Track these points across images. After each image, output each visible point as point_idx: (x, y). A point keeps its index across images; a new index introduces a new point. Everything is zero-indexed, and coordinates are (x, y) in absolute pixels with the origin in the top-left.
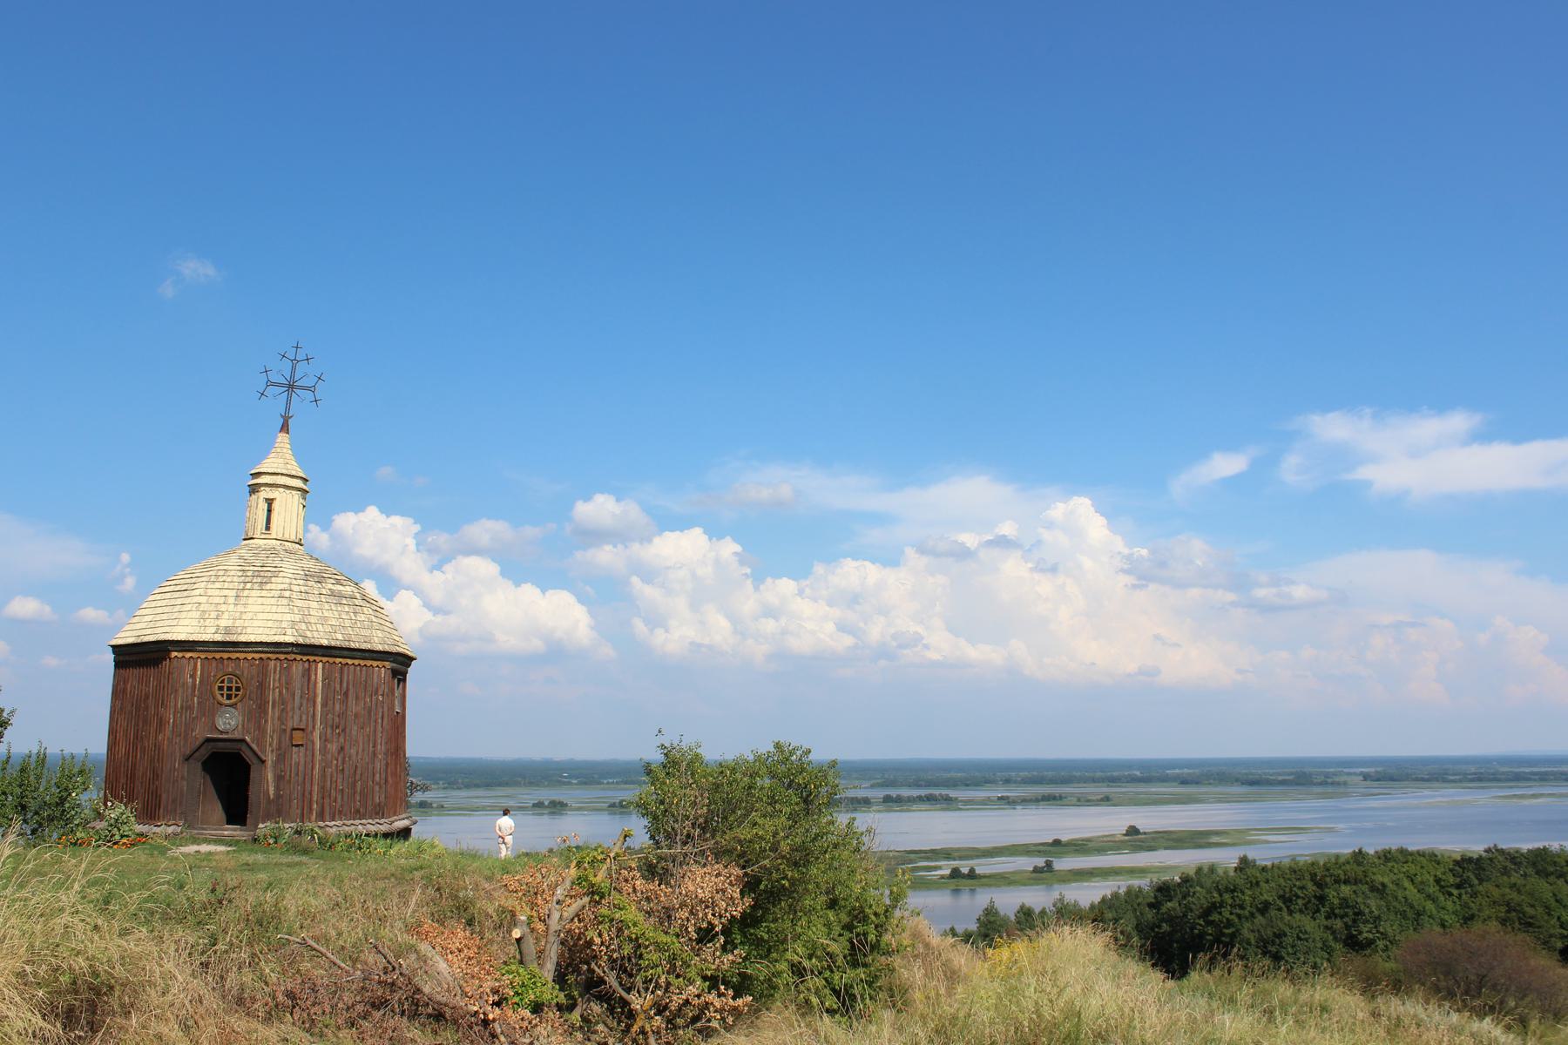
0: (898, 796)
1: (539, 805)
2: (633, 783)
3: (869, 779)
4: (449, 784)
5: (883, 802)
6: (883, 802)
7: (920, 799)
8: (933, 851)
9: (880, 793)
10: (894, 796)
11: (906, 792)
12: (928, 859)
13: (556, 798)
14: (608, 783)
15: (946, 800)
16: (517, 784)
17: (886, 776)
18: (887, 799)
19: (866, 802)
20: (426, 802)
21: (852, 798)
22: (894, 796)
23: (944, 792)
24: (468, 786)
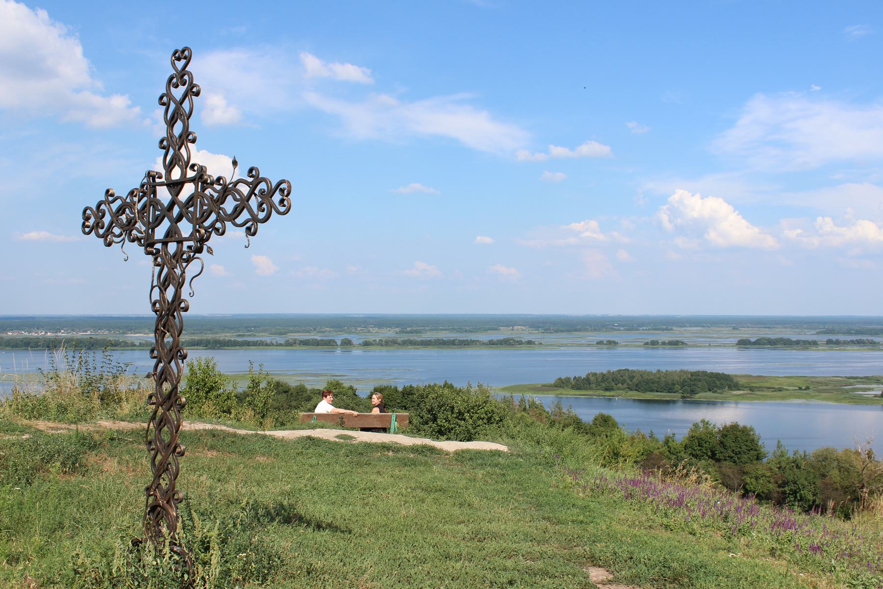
0: (837, 340)
1: (600, 343)
2: (659, 329)
3: (815, 329)
4: (545, 330)
5: (827, 344)
6: (827, 344)
7: (852, 342)
8: (866, 378)
9: (825, 338)
10: (834, 340)
11: (842, 338)
12: (863, 383)
13: (611, 339)
14: (643, 330)
15: (871, 343)
16: (586, 330)
17: (826, 327)
18: (829, 342)
19: (815, 343)
20: (531, 341)
21: (805, 341)
22: (834, 340)
23: (870, 338)
24: (556, 331)
